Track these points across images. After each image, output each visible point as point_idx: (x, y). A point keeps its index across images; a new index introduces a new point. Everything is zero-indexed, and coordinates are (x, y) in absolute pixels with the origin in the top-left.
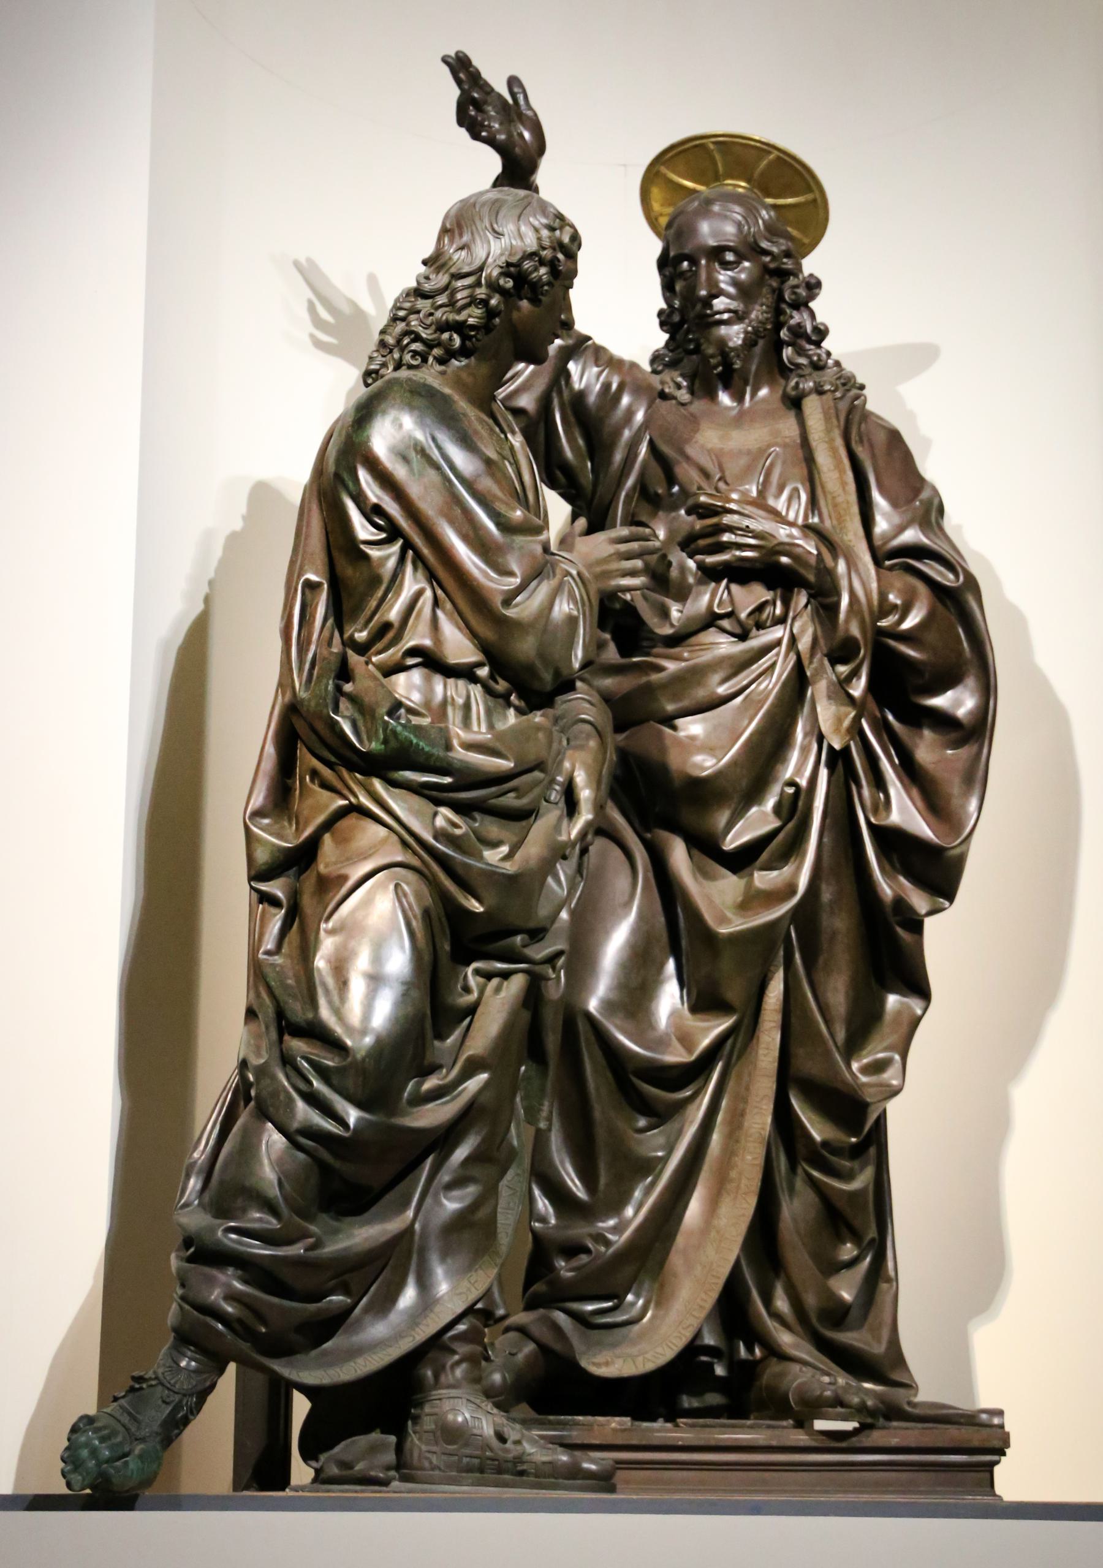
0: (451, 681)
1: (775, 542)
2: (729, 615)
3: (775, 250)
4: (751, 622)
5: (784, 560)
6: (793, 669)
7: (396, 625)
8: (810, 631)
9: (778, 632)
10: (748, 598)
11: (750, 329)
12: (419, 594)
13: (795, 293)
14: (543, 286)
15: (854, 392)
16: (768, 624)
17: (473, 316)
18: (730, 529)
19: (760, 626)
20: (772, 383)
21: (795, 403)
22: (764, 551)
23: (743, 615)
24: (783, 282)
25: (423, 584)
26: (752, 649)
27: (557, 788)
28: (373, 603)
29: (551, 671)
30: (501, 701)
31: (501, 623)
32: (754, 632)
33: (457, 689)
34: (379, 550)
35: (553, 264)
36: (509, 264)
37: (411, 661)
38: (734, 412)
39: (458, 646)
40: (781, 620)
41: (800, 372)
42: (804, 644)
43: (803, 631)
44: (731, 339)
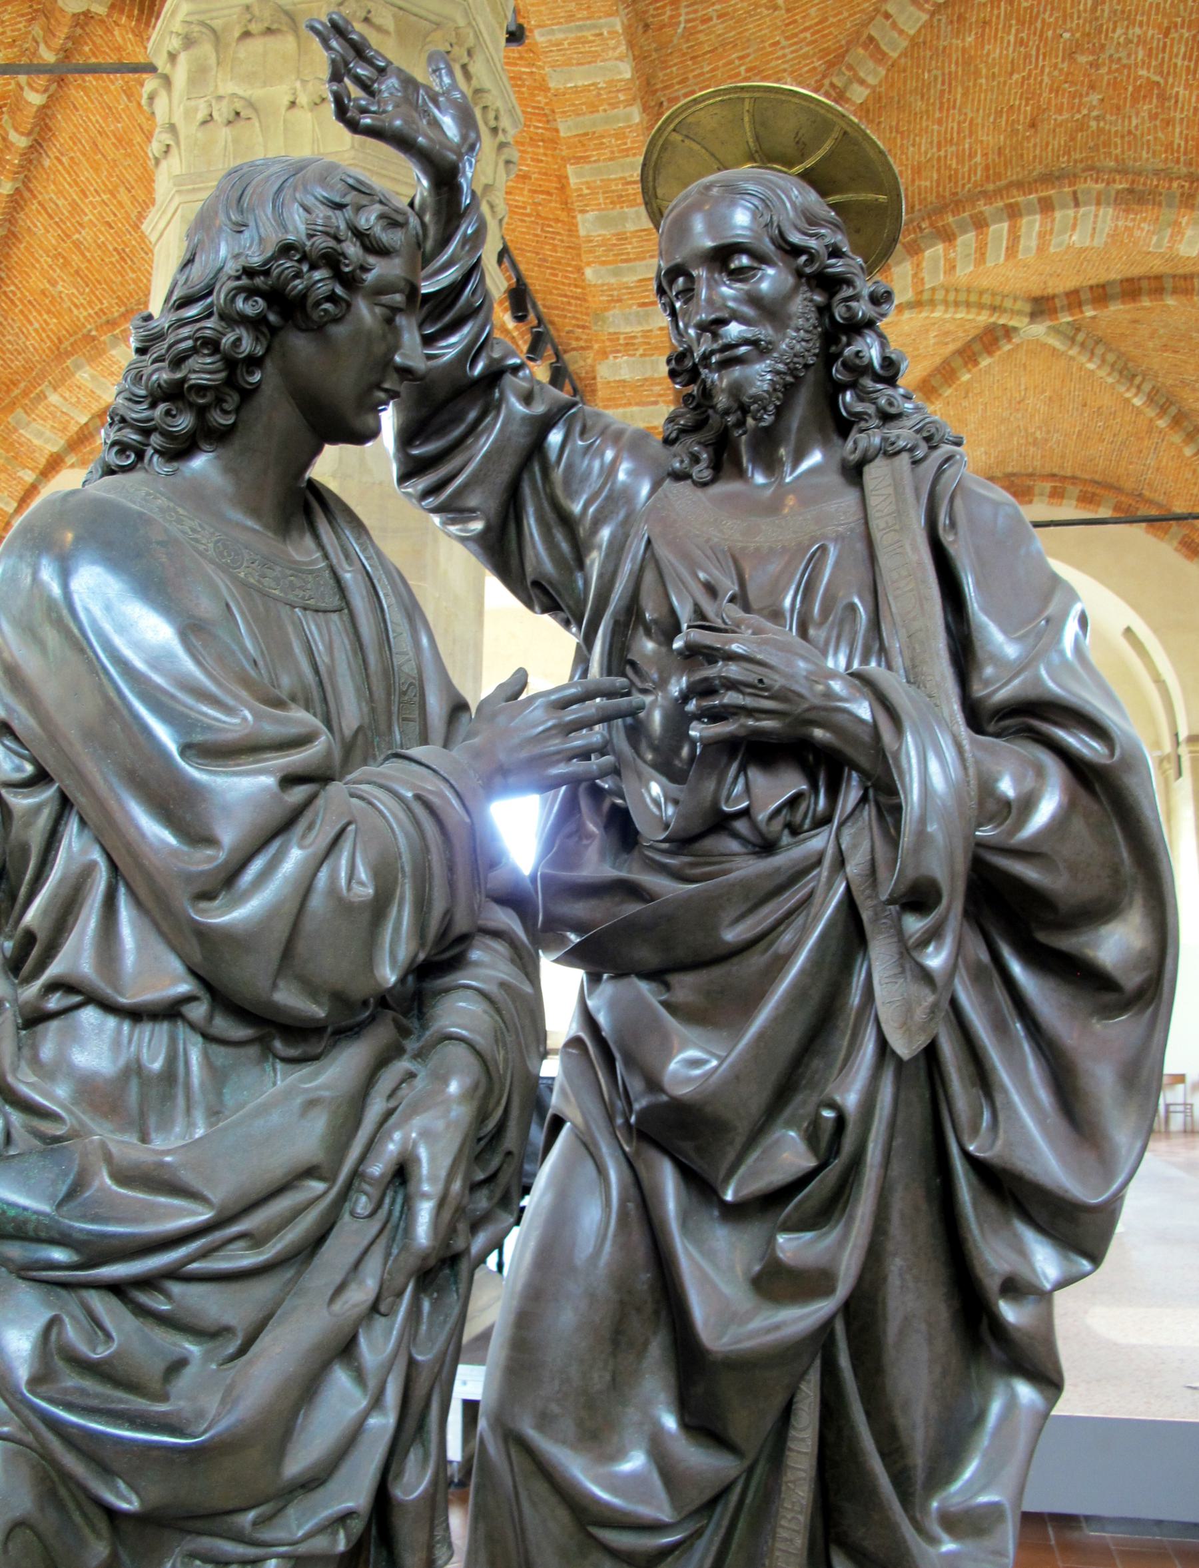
0: (147, 1028)
1: (806, 706)
2: (746, 813)
3: (813, 243)
4: (777, 825)
5: (818, 733)
6: (840, 903)
7: (42, 937)
8: (866, 845)
9: (819, 841)
10: (770, 791)
11: (781, 367)
12: (88, 870)
13: (849, 308)
14: (318, 304)
15: (946, 448)
16: (806, 827)
17: (202, 370)
18: (732, 685)
19: (794, 830)
20: (826, 444)
21: (854, 473)
22: (787, 720)
23: (761, 817)
24: (832, 294)
25: (97, 855)
26: (778, 870)
27: (366, 1187)
28: (23, 890)
29: (325, 999)
30: (253, 1051)
31: (203, 934)
32: (786, 839)
33: (151, 1046)
34: (26, 796)
35: (332, 260)
36: (249, 272)
37: (54, 1002)
38: (769, 492)
39: (151, 968)
40: (826, 820)
41: (863, 425)
42: (855, 867)
43: (855, 846)
44: (752, 384)
